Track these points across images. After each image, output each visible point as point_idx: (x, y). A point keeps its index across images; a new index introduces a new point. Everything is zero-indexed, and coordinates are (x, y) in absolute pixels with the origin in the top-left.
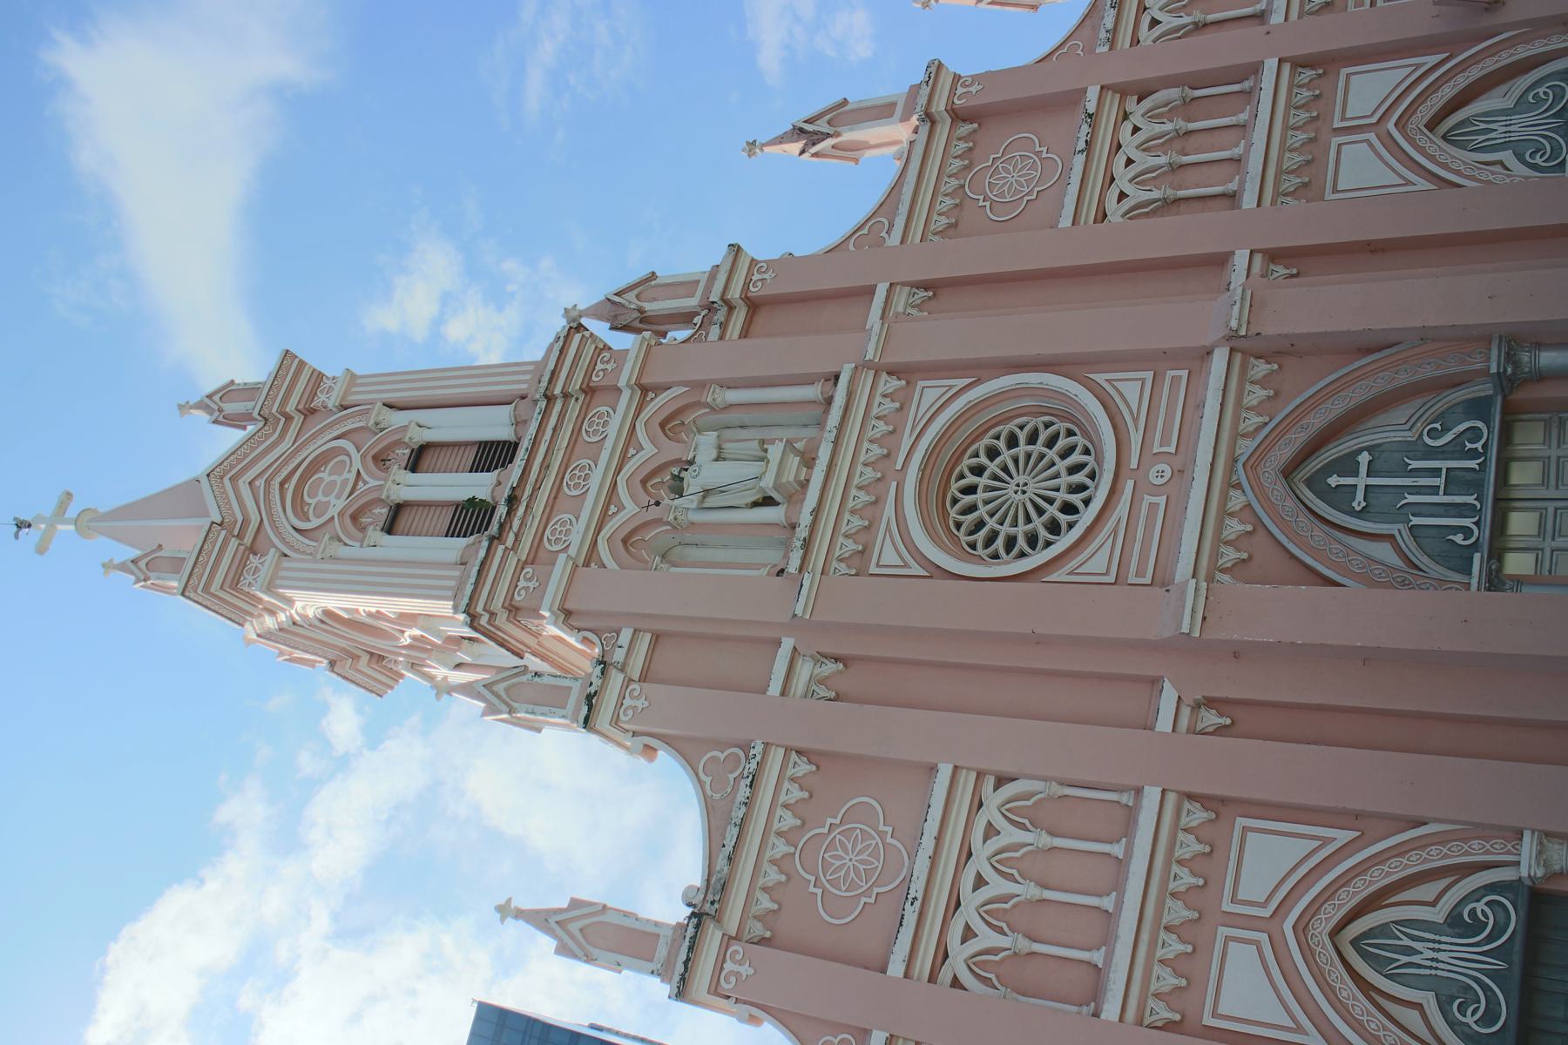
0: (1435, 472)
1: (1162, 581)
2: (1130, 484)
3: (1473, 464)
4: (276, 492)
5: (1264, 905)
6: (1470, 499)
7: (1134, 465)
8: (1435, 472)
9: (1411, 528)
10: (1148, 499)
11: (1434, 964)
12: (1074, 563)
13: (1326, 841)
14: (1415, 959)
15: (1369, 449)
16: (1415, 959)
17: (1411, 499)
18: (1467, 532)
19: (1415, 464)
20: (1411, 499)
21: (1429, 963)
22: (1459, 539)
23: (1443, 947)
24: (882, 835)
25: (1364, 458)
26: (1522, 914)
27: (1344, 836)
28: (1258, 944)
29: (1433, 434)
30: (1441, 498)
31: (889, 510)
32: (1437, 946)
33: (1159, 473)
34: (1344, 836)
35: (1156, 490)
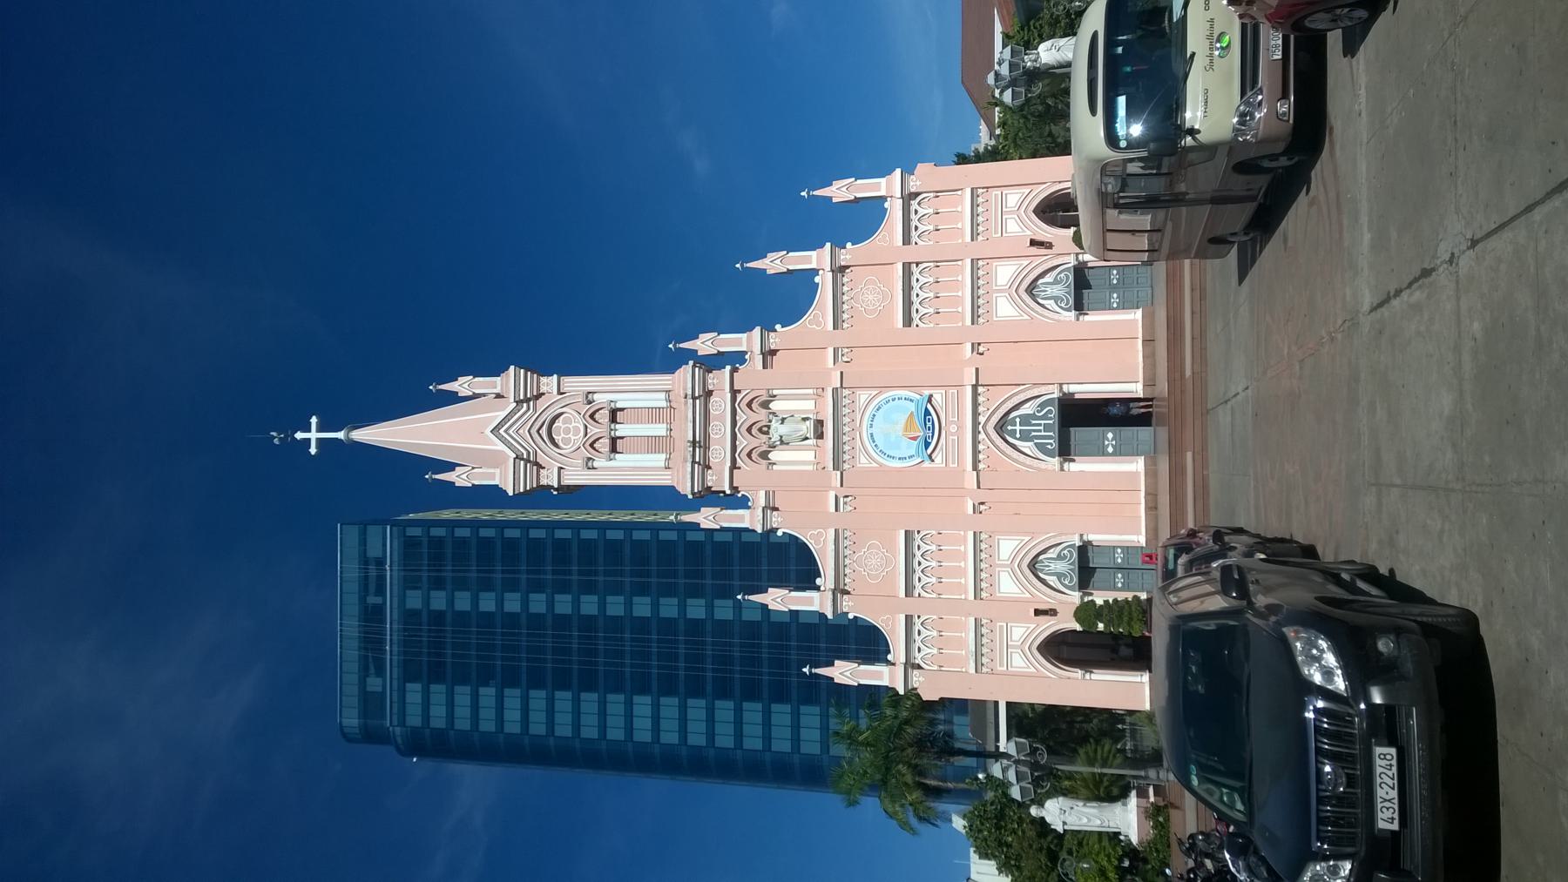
0: (1040, 425)
3: (1051, 422)
4: (536, 436)
6: (1051, 434)
8: (1040, 425)
9: (1035, 444)
15: (1019, 416)
17: (1034, 434)
18: (1051, 445)
19: (1034, 422)
20: (1034, 434)
22: (1049, 447)
24: (883, 553)
25: (1018, 420)
27: (1027, 539)
28: (1008, 572)
29: (1038, 411)
30: (1043, 433)
33: (953, 428)
35: (952, 434)
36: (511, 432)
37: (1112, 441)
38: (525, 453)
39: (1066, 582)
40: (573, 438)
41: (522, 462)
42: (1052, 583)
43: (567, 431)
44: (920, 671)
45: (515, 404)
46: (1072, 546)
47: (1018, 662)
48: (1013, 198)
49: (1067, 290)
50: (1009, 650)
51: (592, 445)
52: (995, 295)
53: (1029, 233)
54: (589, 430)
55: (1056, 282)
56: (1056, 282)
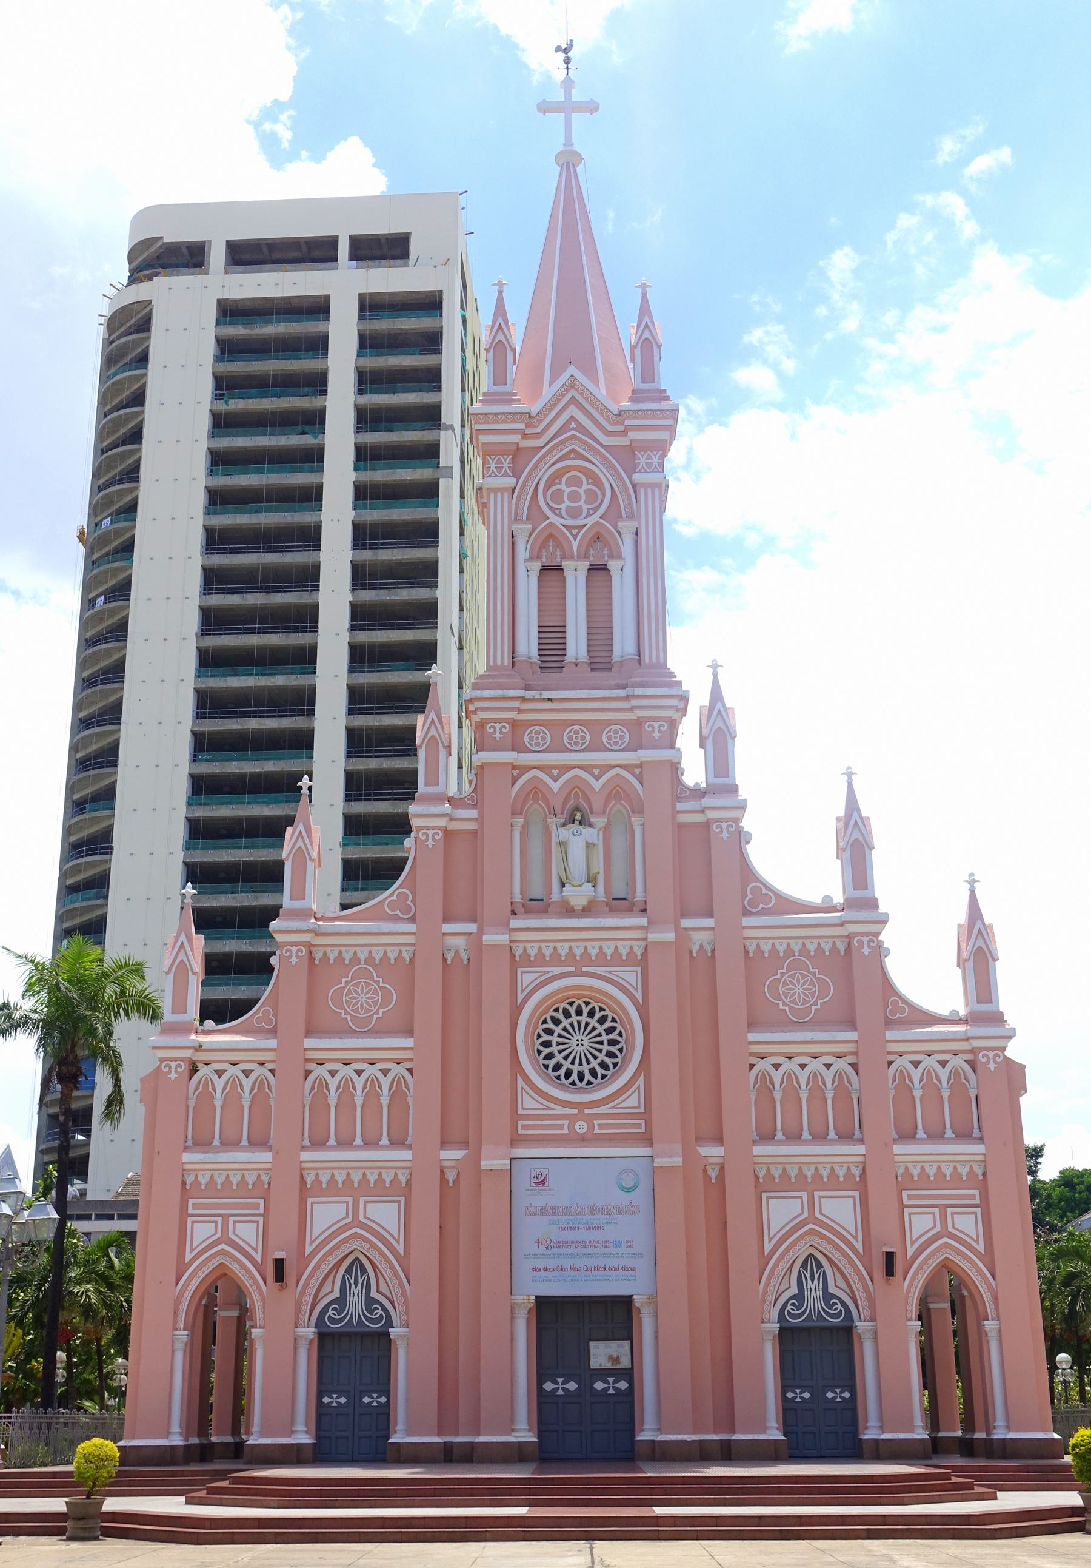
1: (516, 1140)
2: (575, 1111)
5: (365, 1216)
7: (587, 1111)
10: (566, 1123)
11: (352, 1295)
12: (528, 1089)
13: (398, 1241)
14: (353, 1286)
16: (353, 1286)
21: (352, 1292)
23: (360, 1297)
26: (380, 1330)
31: (556, 971)
32: (360, 1295)
33: (581, 1127)
34: (400, 1249)
35: (571, 1127)
36: (572, 407)
37: (564, 1389)
38: (538, 430)
39: (330, 1312)
40: (563, 507)
41: (522, 426)
42: (327, 1288)
43: (574, 497)
44: (187, 1074)
45: (616, 412)
46: (390, 1323)
47: (201, 1233)
48: (967, 1224)
49: (815, 1316)
50: (219, 1219)
51: (551, 536)
52: (804, 1195)
53: (910, 1251)
54: (575, 532)
55: (828, 1297)
56: (828, 1297)
